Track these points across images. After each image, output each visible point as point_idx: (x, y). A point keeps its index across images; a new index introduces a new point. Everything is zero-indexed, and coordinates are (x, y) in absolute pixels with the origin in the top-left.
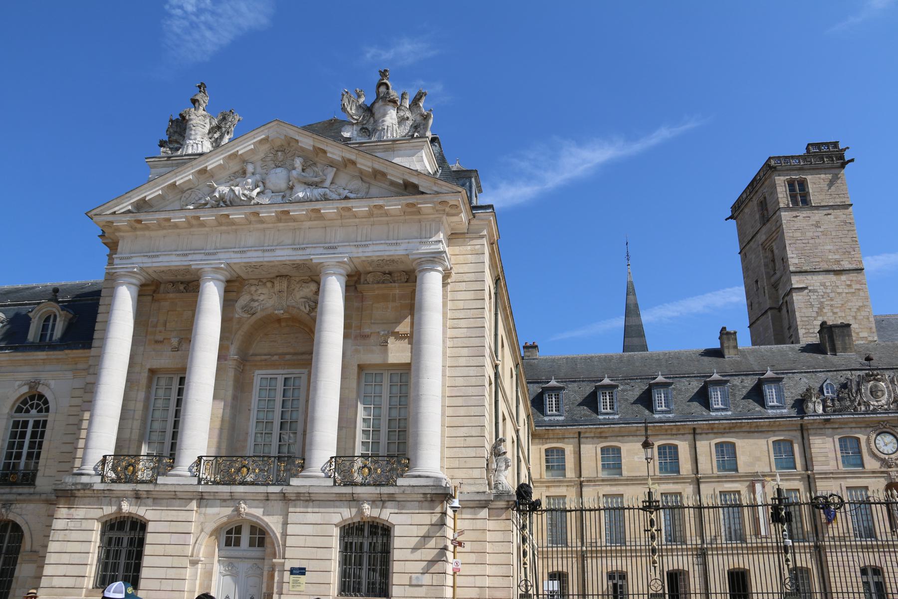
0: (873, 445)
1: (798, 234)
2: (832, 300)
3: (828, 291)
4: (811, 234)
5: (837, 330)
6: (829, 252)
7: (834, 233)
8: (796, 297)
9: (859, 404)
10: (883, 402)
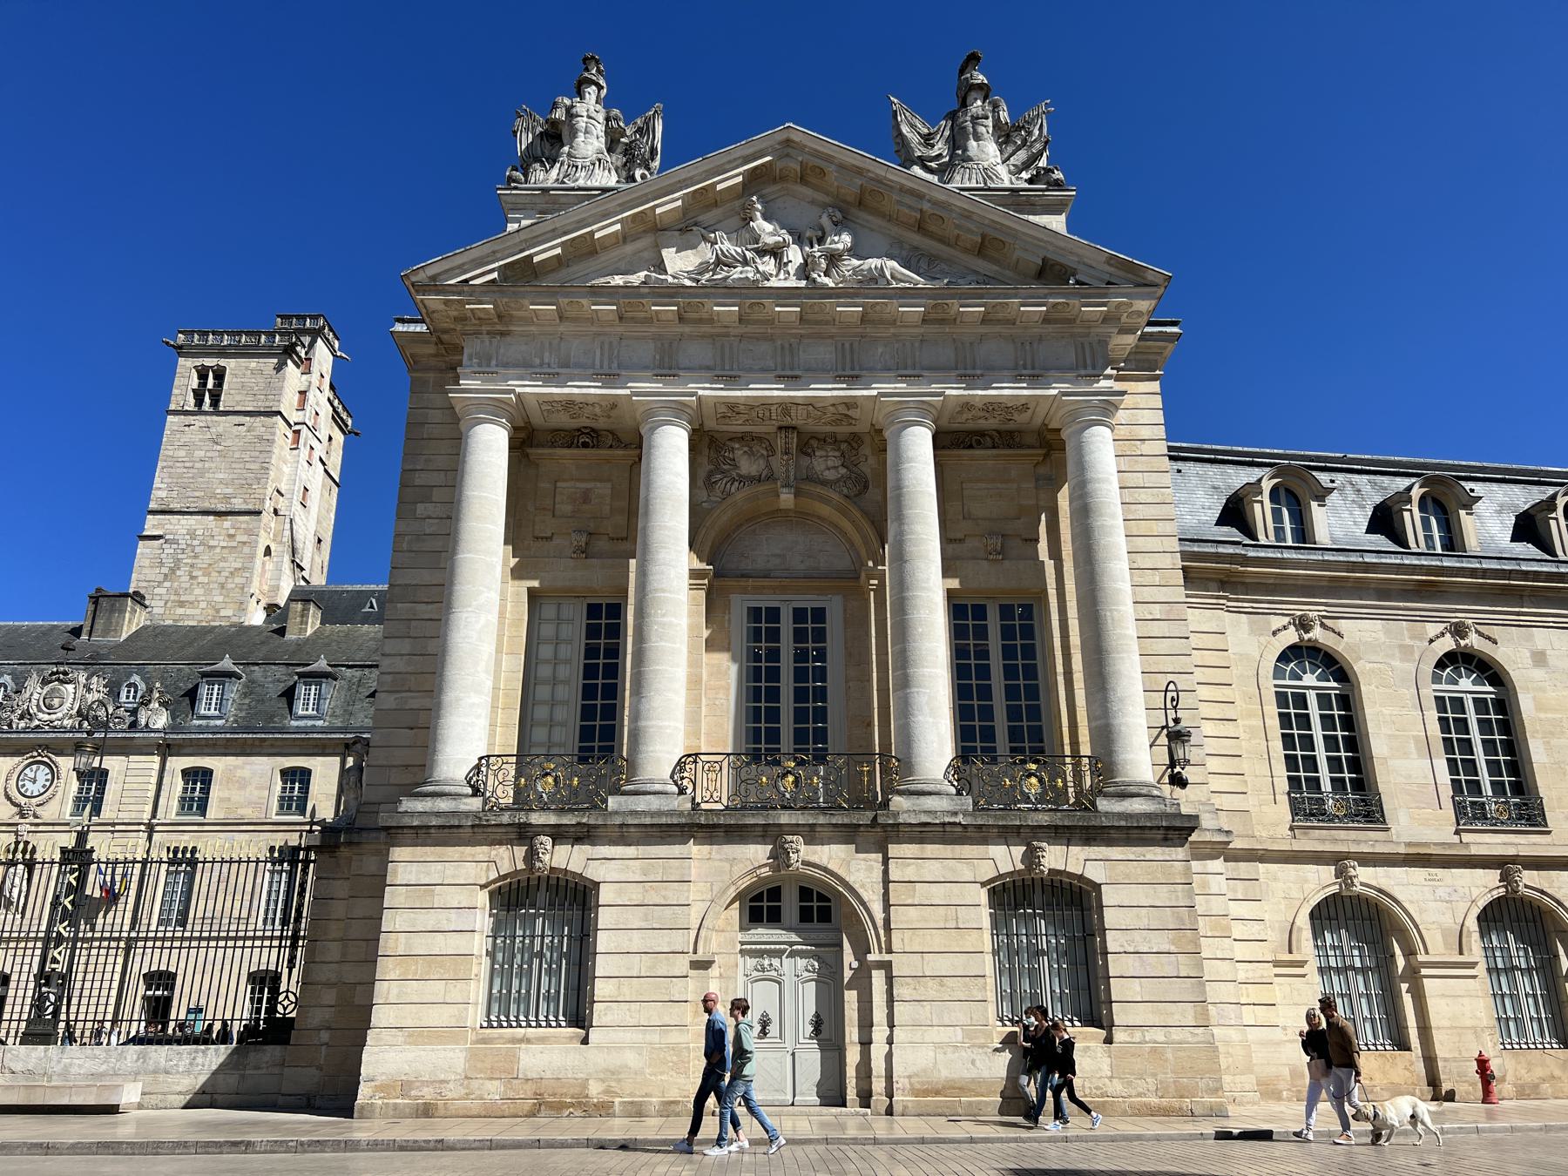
0: (13, 782)
1: (182, 453)
2: (196, 557)
3: (196, 543)
4: (202, 453)
5: (104, 603)
6: (220, 485)
7: (237, 455)
8: (143, 548)
9: (21, 717)
10: (60, 715)
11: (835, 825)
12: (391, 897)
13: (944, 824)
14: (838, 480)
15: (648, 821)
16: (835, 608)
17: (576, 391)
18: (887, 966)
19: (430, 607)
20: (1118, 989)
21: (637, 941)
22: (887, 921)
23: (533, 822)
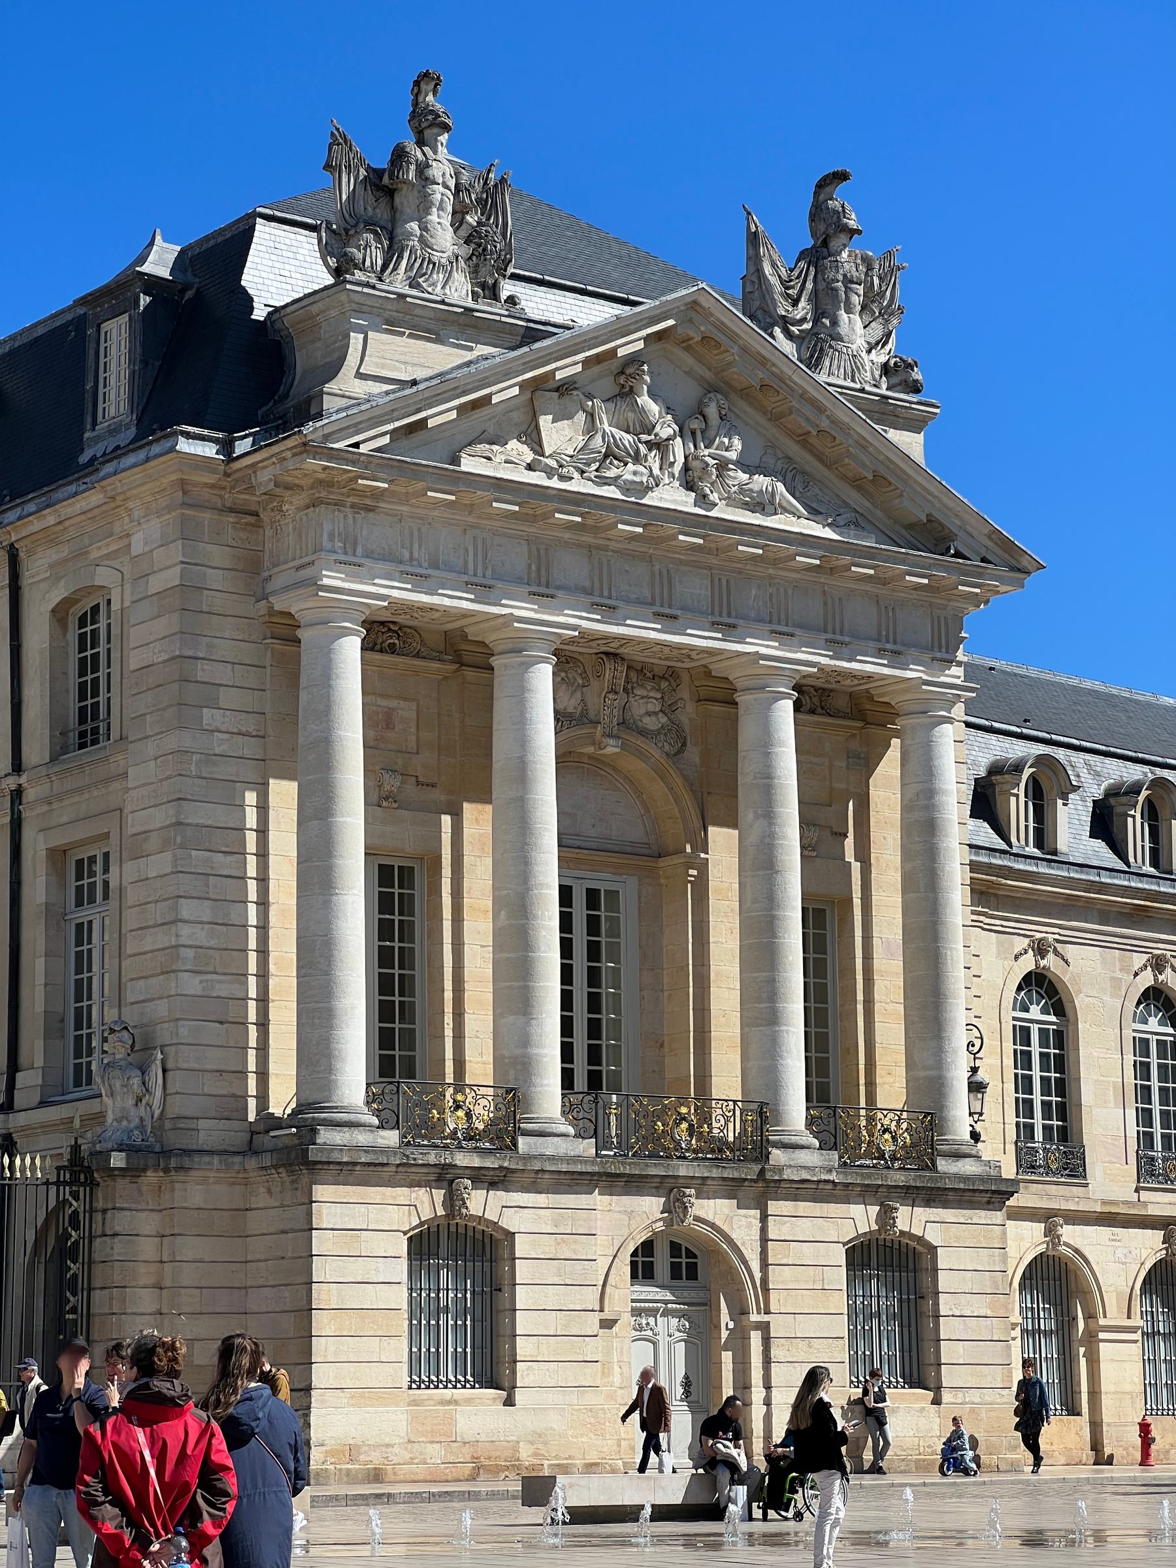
11: (724, 1179)
12: (320, 1242)
13: (819, 1181)
14: (659, 732)
15: (564, 1168)
16: (628, 890)
17: (447, 602)
18: (764, 1327)
19: (229, 858)
20: (947, 1352)
21: (552, 1297)
22: (765, 1281)
23: (458, 1163)
